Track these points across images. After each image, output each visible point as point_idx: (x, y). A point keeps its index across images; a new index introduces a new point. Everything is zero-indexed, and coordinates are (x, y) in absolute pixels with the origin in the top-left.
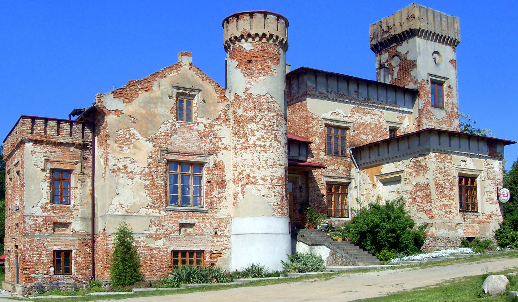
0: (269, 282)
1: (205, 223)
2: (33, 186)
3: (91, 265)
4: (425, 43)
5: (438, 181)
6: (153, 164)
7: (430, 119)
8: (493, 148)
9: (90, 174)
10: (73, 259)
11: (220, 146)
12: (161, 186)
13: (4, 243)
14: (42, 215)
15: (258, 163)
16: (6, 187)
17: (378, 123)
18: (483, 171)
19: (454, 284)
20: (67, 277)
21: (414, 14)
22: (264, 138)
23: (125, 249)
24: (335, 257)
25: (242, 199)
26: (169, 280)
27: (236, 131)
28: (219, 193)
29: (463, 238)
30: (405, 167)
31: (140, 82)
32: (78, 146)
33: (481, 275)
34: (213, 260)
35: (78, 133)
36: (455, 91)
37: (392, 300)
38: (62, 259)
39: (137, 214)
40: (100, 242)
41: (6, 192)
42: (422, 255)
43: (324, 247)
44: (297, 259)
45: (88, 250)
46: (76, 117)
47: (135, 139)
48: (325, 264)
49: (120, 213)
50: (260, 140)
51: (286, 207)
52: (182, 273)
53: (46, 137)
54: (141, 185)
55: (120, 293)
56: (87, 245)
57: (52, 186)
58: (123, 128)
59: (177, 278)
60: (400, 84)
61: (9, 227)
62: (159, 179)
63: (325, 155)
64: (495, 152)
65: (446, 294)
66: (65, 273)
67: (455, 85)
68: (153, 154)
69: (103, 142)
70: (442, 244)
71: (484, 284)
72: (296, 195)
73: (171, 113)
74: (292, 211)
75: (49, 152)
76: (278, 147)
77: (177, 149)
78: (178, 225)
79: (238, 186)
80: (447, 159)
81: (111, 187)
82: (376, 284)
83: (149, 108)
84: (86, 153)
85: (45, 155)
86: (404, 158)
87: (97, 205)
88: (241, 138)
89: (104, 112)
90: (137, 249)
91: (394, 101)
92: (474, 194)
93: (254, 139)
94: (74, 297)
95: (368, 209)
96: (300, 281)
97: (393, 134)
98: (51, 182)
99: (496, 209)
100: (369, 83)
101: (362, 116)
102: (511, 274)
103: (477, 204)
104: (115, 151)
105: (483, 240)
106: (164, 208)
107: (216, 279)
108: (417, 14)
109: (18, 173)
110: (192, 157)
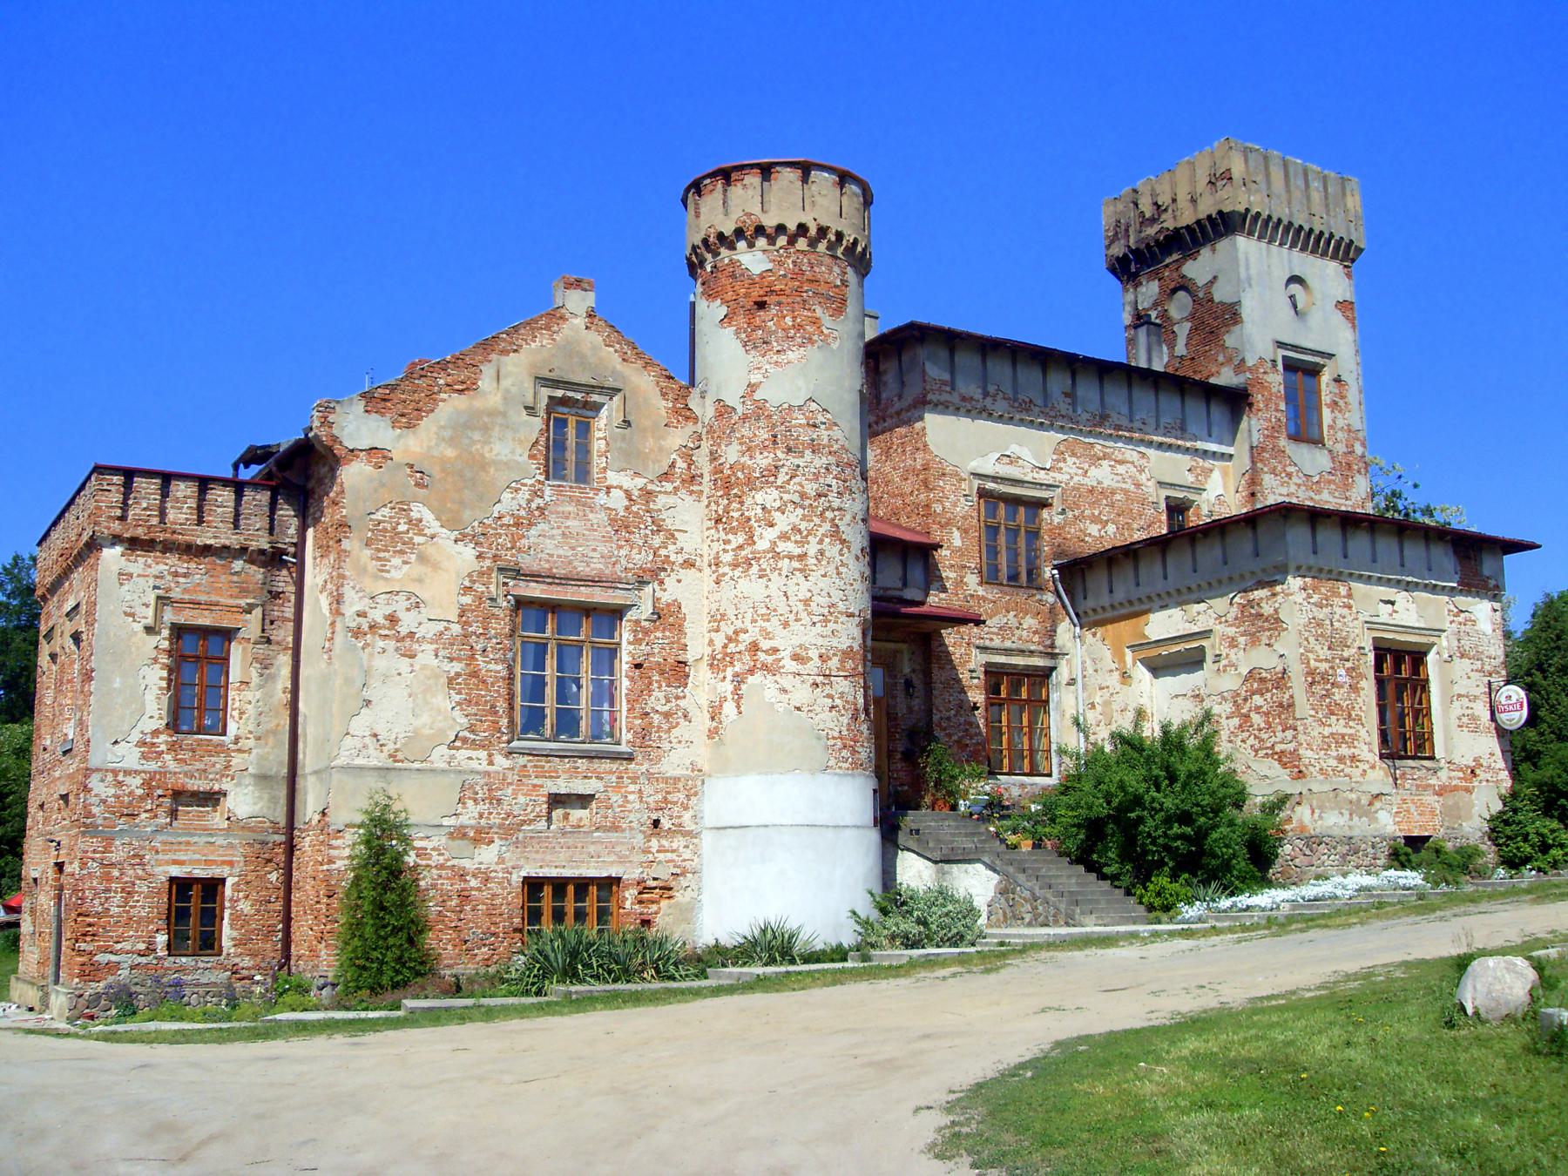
0: (814, 980)
1: (626, 792)
2: (118, 680)
3: (281, 926)
4: (1264, 253)
5: (1312, 663)
6: (473, 611)
7: (1283, 475)
8: (1473, 563)
9: (288, 643)
10: (227, 904)
11: (672, 558)
12: (496, 677)
13: (23, 854)
14: (140, 768)
15: (783, 609)
16: (38, 680)
17: (1132, 488)
18: (1444, 631)
19: (1372, 987)
20: (207, 962)
21: (1229, 170)
22: (800, 531)
23: (384, 873)
24: (1013, 899)
25: (736, 717)
26: (514, 972)
27: (721, 512)
28: (668, 701)
29: (1395, 839)
30: (1216, 619)
31: (443, 366)
32: (255, 556)
33: (1451, 957)
34: (645, 907)
35: (257, 519)
36: (1353, 394)
37: (1187, 1036)
38: (195, 905)
39: (424, 764)
40: (309, 853)
41: (38, 696)
42: (1273, 892)
43: (979, 866)
44: (897, 907)
45: (274, 877)
46: (255, 469)
47: (425, 535)
48: (982, 921)
49: (374, 763)
50: (789, 539)
51: (865, 744)
52: (553, 950)
53: (165, 530)
54: (437, 677)
55: (363, 1015)
56: (269, 861)
57: (173, 677)
58: (390, 502)
59: (538, 965)
60: (1195, 372)
61: (42, 806)
62: (491, 656)
63: (981, 584)
64: (1477, 573)
65: (1348, 1017)
66: (201, 950)
67: (1354, 375)
68: (474, 582)
69: (331, 543)
70: (1332, 857)
71: (1461, 985)
72: (895, 707)
73: (532, 457)
74: (884, 755)
75: (170, 573)
76: (841, 561)
77: (547, 566)
78: (545, 799)
79: (724, 678)
80: (1338, 595)
81: (348, 681)
82: (1138, 986)
83: (467, 441)
84: (277, 579)
85: (159, 582)
86: (1211, 594)
87: (305, 736)
88: (734, 531)
89: (334, 455)
90: (419, 874)
91: (1178, 421)
92: (1420, 703)
93: (771, 534)
94: (224, 1025)
95: (1108, 748)
96: (907, 974)
97: (1178, 520)
98: (173, 665)
99: (1488, 748)
100: (1104, 370)
101: (1086, 466)
102: (1542, 952)
103: (1431, 733)
104: (362, 571)
105: (1454, 846)
106: (504, 745)
107: (655, 968)
108: (1238, 169)
109: (76, 638)
110: (590, 589)
